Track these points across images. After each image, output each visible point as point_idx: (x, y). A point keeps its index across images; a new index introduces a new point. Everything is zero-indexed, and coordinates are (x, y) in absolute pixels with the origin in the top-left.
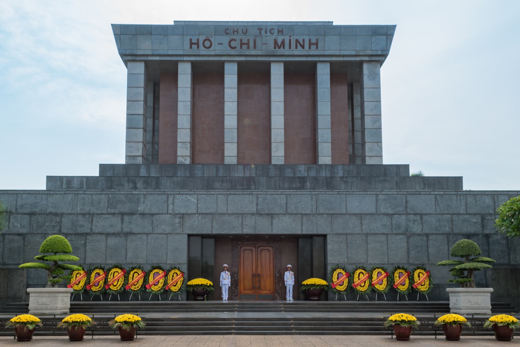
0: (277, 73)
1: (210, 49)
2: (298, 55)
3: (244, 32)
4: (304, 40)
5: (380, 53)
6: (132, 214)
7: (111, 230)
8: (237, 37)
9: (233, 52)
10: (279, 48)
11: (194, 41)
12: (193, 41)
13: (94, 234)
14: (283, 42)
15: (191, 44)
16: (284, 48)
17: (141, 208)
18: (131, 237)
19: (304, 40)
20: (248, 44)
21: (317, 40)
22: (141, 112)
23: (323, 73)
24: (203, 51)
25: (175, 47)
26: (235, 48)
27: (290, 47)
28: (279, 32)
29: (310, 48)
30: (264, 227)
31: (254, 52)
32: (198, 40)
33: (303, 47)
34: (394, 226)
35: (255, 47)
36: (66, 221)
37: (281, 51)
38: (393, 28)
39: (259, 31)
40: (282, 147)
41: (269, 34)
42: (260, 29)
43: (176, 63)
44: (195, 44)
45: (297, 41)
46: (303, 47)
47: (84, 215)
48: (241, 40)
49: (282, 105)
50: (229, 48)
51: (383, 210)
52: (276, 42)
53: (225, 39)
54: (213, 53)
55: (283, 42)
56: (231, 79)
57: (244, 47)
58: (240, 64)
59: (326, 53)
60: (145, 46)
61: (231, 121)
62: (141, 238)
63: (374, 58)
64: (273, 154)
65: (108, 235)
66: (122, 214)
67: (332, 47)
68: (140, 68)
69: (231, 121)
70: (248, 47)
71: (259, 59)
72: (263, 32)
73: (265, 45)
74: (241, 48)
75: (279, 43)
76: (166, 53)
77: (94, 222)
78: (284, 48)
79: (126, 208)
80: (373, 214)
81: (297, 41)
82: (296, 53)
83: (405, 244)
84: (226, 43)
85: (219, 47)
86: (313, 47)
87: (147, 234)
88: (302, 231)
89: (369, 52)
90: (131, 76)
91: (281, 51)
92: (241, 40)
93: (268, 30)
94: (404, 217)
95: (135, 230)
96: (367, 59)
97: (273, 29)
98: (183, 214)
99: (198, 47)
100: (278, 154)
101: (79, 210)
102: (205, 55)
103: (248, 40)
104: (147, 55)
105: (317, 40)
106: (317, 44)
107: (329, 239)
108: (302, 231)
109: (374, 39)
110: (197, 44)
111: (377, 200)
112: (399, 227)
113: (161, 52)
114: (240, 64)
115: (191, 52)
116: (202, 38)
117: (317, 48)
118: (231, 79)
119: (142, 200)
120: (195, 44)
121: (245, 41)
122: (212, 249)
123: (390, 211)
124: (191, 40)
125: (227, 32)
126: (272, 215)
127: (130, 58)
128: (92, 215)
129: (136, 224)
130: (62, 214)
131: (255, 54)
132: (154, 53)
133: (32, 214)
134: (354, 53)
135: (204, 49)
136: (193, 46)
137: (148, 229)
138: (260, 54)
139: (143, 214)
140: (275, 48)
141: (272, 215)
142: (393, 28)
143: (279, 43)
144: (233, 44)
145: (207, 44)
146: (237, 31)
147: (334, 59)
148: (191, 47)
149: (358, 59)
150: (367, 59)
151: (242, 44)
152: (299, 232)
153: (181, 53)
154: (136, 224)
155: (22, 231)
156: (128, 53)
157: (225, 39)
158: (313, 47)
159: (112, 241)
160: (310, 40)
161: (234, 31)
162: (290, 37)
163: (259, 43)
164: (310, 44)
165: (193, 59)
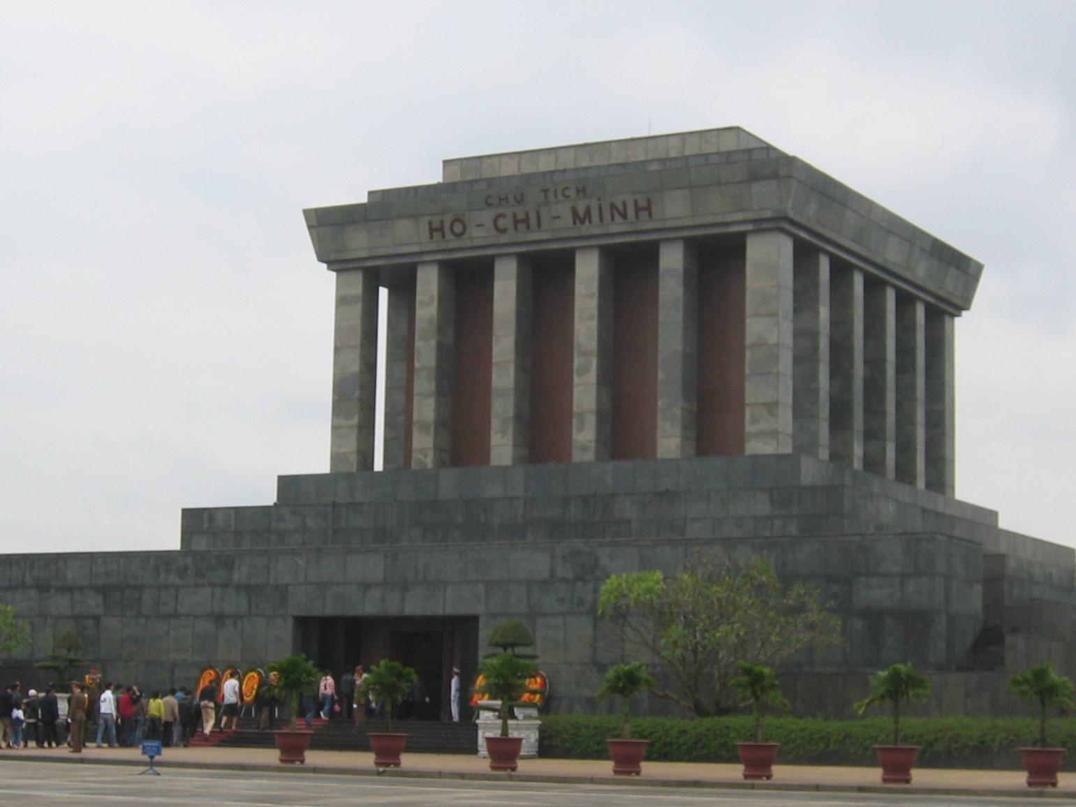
0: (587, 270)
1: (463, 237)
2: (619, 231)
3: (518, 199)
4: (624, 204)
5: (768, 214)
6: (225, 585)
8: (508, 211)
9: (504, 239)
10: (582, 222)
11: (436, 225)
12: (434, 226)
13: (179, 615)
14: (588, 212)
15: (432, 230)
16: (590, 222)
19: (624, 204)
20: (526, 221)
21: (649, 201)
23: (672, 259)
25: (407, 237)
26: (504, 231)
27: (601, 219)
28: (578, 191)
29: (637, 216)
30: (395, 605)
31: (537, 236)
32: (442, 222)
33: (624, 216)
34: (575, 601)
35: (539, 225)
36: (147, 597)
37: (586, 229)
39: (542, 195)
40: (591, 421)
41: (560, 197)
42: (545, 191)
44: (436, 230)
45: (613, 206)
46: (624, 216)
47: (167, 587)
48: (515, 216)
50: (494, 232)
51: (560, 573)
52: (575, 214)
53: (487, 217)
54: (468, 244)
55: (588, 212)
57: (520, 226)
59: (669, 224)
60: (359, 243)
62: (235, 623)
63: (764, 226)
64: (574, 437)
65: (195, 617)
67: (675, 209)
68: (356, 284)
69: (503, 374)
70: (528, 227)
71: (552, 246)
72: (551, 195)
73: (557, 220)
74: (516, 228)
75: (581, 211)
76: (391, 251)
77: (180, 597)
78: (590, 222)
80: (545, 582)
81: (613, 206)
82: (615, 229)
83: (588, 630)
84: (490, 224)
85: (479, 234)
86: (644, 214)
87: (241, 617)
88: (444, 609)
89: (750, 216)
90: (342, 302)
91: (586, 229)
92: (515, 216)
93: (559, 192)
94: (591, 585)
96: (750, 227)
97: (567, 188)
98: (287, 585)
99: (443, 236)
103: (527, 214)
104: (364, 259)
105: (649, 201)
106: (648, 209)
107: (482, 623)
108: (444, 609)
109: (757, 188)
110: (441, 230)
111: (553, 557)
112: (581, 602)
113: (382, 252)
115: (432, 247)
116: (448, 220)
117: (650, 215)
119: (236, 566)
120: (436, 230)
121: (521, 216)
122: (334, 639)
123: (570, 575)
124: (430, 223)
125: (490, 201)
126: (404, 587)
127: (337, 266)
128: (177, 588)
130: (140, 588)
132: (374, 253)
134: (719, 219)
135: (452, 237)
136: (435, 234)
138: (550, 237)
139: (238, 588)
140: (575, 223)
143: (581, 211)
144: (502, 223)
145: (458, 228)
146: (506, 198)
147: (686, 233)
148: (432, 238)
149: (733, 229)
150: (750, 227)
151: (516, 222)
152: (440, 612)
153: (416, 249)
156: (333, 257)
157: (487, 217)
158: (644, 214)
160: (636, 203)
161: (501, 200)
162: (599, 199)
163: (545, 216)
164: (638, 210)
165: (440, 257)
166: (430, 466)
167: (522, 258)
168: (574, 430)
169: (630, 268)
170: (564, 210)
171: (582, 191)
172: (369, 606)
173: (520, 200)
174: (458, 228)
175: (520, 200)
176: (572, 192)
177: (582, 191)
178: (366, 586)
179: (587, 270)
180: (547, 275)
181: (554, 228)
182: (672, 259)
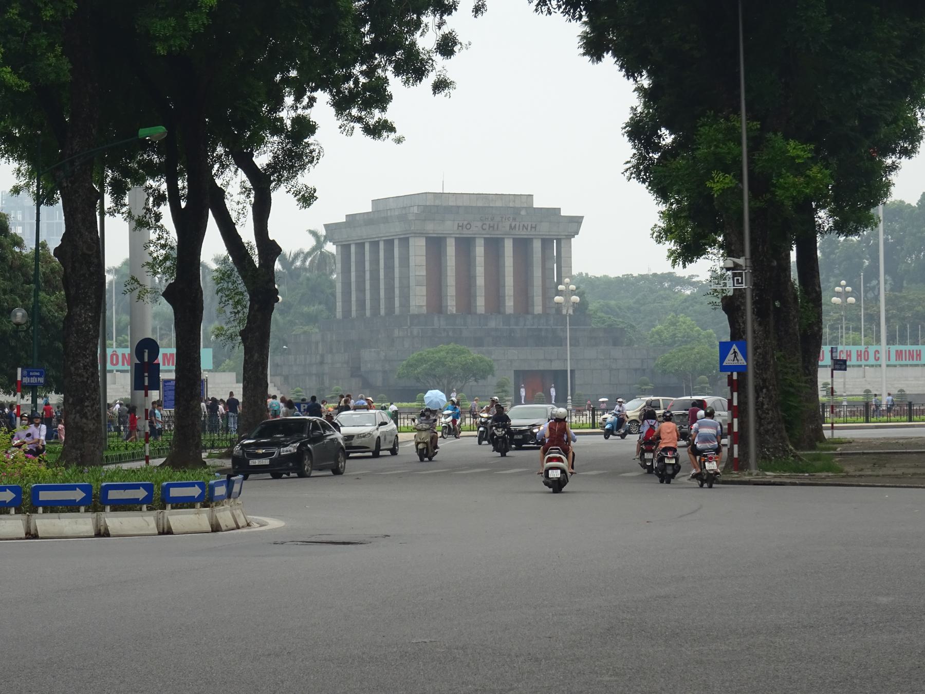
8: (488, 223)
20: (493, 227)
22: (424, 273)
38: (582, 217)
40: (512, 298)
43: (445, 238)
49: (512, 269)
52: (511, 226)
56: (480, 250)
58: (485, 238)
60: (431, 228)
61: (480, 281)
69: (480, 281)
100: (509, 304)
102: (466, 233)
114: (485, 238)
116: (465, 223)
118: (480, 250)
126: (551, 361)
131: (496, 234)
141: (551, 361)
142: (582, 217)
144: (484, 227)
157: (479, 224)
167: (487, 240)
168: (507, 301)
169: (523, 246)
170: (507, 224)
171: (514, 219)
172: (542, 366)
173: (492, 220)
174: (468, 226)
175: (492, 220)
177: (514, 219)
179: (509, 246)
180: (494, 246)
182: (537, 245)
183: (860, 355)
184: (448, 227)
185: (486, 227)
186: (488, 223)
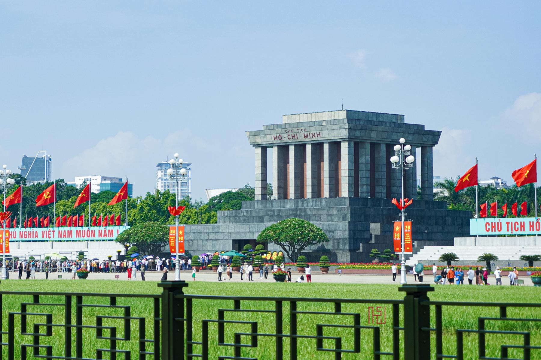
7: (213, 238)
8: (290, 134)
17: (220, 230)
18: (218, 241)
20: (294, 137)
24: (279, 141)
31: (298, 141)
36: (202, 235)
65: (213, 240)
66: (216, 232)
79: (216, 230)
85: (285, 139)
86: (319, 136)
91: (308, 139)
95: (219, 238)
101: (205, 231)
116: (278, 135)
129: (219, 236)
133: (194, 233)
137: (222, 238)
144: (290, 137)
154: (219, 236)
155: (192, 239)
157: (286, 135)
158: (319, 136)
159: (214, 242)
166: (277, 199)
176: (303, 130)
178: (246, 232)
181: (301, 139)
183: (533, 226)
184: (268, 139)
185: (290, 137)
186: (290, 134)
